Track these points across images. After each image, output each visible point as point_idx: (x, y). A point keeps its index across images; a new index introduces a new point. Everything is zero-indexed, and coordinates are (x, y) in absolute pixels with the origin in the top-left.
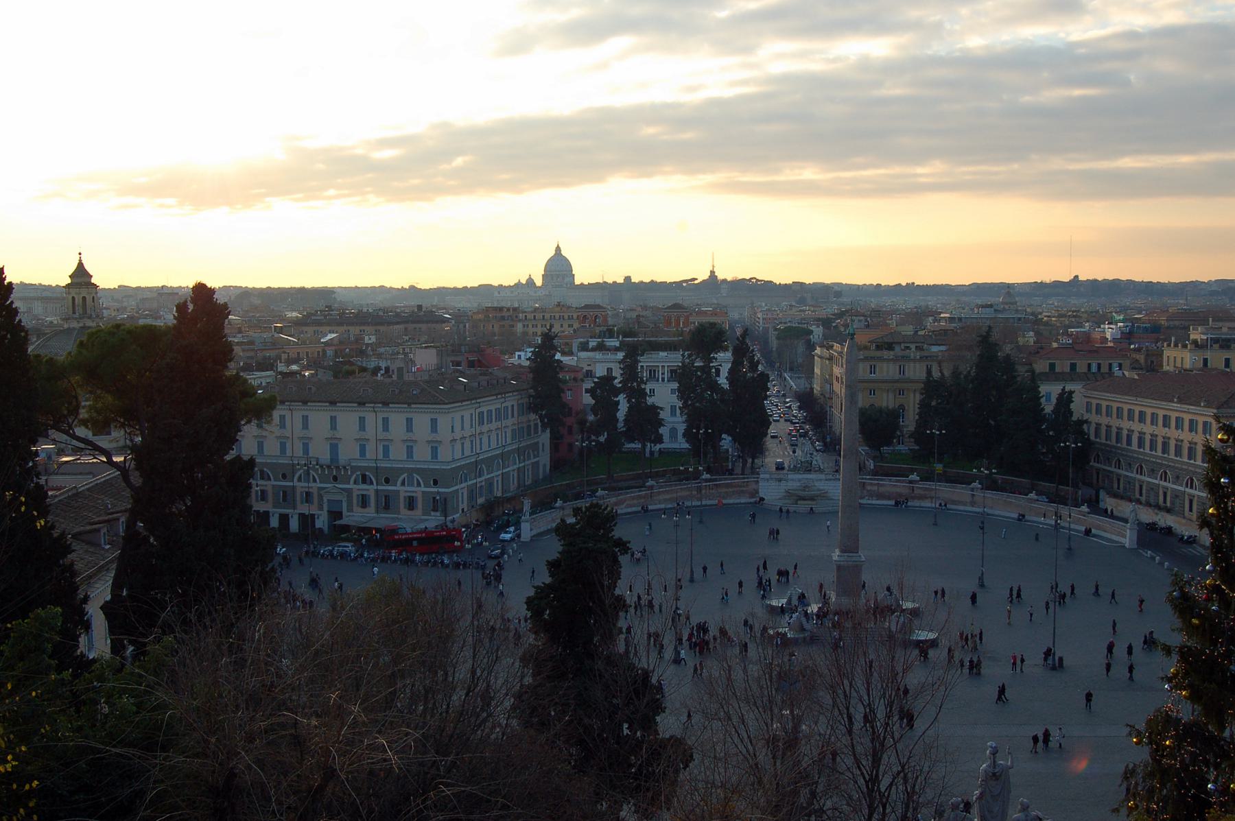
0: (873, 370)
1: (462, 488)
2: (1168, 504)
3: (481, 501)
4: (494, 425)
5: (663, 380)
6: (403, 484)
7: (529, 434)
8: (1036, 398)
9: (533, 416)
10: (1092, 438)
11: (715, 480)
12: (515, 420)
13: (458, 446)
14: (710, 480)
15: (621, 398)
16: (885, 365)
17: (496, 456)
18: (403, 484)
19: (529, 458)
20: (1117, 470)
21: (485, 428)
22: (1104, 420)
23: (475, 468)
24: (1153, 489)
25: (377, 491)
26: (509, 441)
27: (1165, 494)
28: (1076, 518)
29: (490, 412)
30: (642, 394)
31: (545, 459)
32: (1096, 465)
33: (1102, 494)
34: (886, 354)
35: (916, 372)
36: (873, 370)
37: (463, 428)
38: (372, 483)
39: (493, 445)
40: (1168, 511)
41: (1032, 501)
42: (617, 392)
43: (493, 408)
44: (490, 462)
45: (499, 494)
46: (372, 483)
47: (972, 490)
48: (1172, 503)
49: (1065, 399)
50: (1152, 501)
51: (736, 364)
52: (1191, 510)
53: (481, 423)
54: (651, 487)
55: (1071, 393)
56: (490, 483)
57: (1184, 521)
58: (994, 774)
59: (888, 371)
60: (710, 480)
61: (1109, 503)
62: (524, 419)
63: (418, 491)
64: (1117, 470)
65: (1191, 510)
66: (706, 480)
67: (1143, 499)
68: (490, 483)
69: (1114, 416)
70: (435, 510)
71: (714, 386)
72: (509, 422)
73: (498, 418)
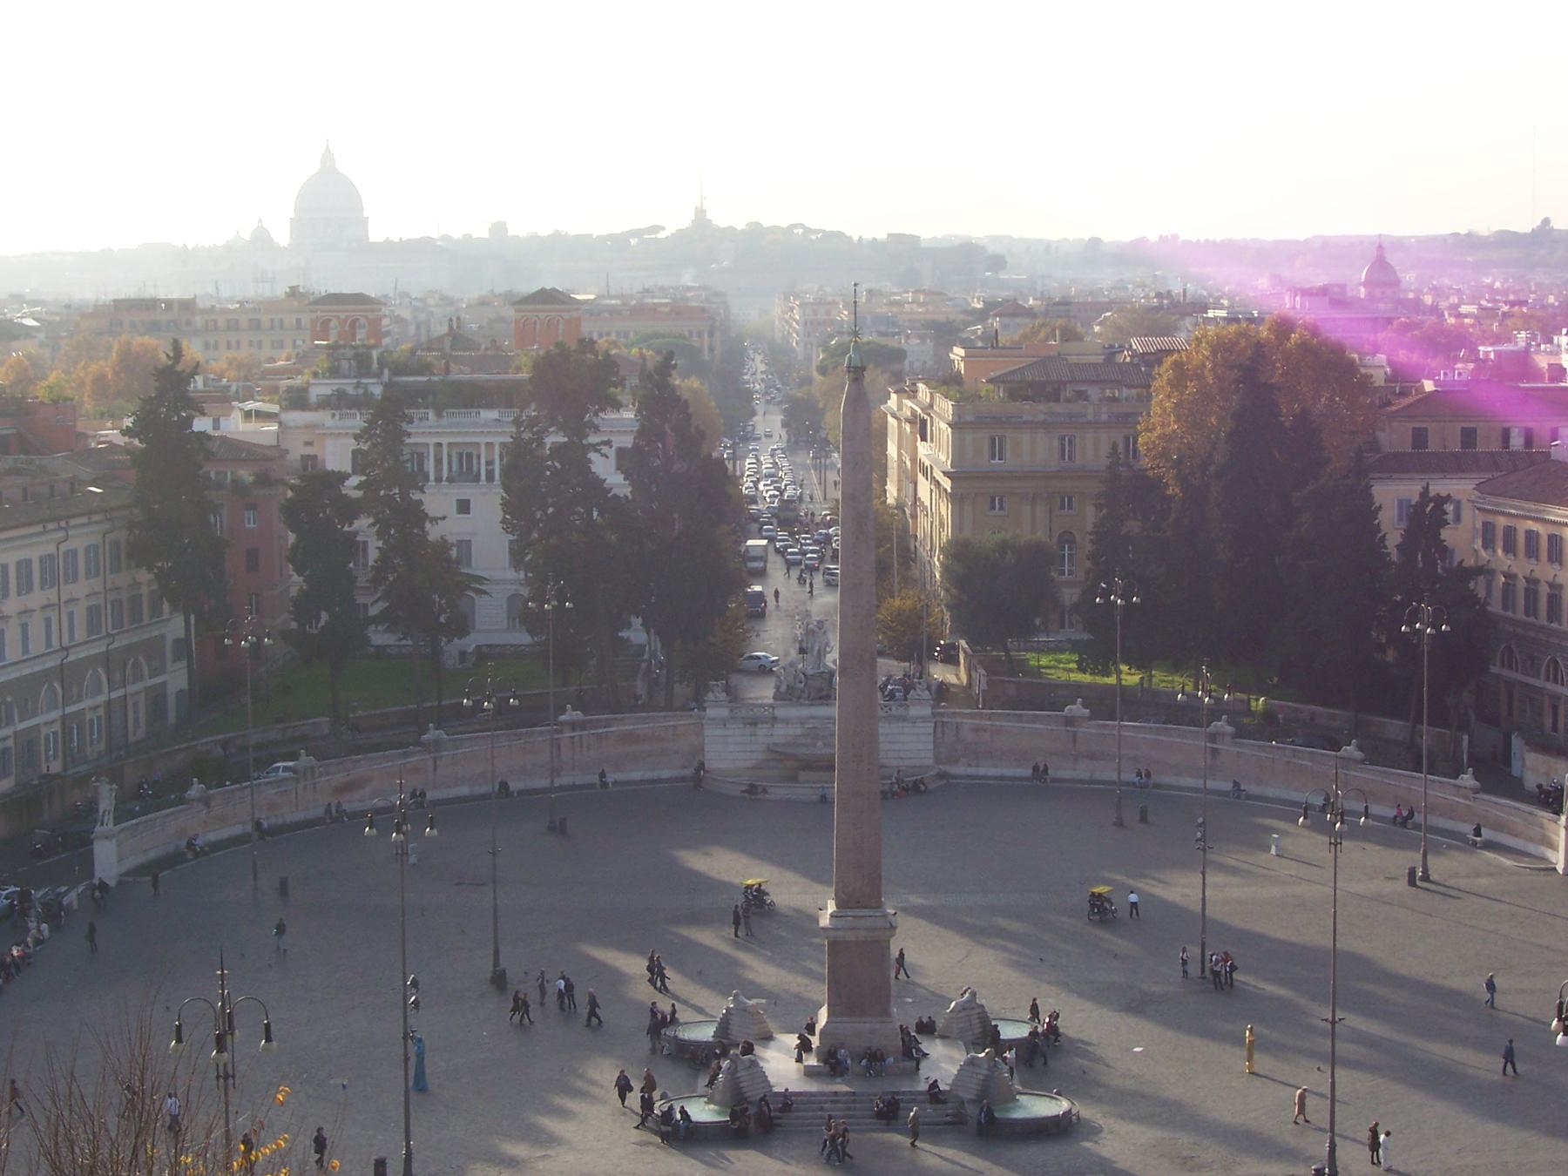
4: (37, 598)
5: (490, 477)
8: (1367, 512)
9: (144, 576)
10: (1495, 607)
12: (96, 584)
14: (582, 725)
15: (363, 523)
17: (45, 675)
19: (138, 677)
20: (1550, 686)
22: (1521, 567)
26: (80, 634)
29: (23, 566)
30: (415, 516)
31: (176, 679)
32: (1506, 672)
33: (1517, 742)
35: (1093, 451)
39: (37, 646)
41: (1348, 760)
42: (351, 510)
43: (35, 554)
45: (56, 767)
47: (1213, 738)
49: (1427, 519)
51: (647, 432)
54: (437, 745)
55: (1441, 501)
60: (582, 725)
61: (1533, 767)
64: (1550, 686)
66: (574, 725)
68: (28, 742)
69: (1544, 555)
71: (596, 487)
72: (81, 588)
73: (49, 580)
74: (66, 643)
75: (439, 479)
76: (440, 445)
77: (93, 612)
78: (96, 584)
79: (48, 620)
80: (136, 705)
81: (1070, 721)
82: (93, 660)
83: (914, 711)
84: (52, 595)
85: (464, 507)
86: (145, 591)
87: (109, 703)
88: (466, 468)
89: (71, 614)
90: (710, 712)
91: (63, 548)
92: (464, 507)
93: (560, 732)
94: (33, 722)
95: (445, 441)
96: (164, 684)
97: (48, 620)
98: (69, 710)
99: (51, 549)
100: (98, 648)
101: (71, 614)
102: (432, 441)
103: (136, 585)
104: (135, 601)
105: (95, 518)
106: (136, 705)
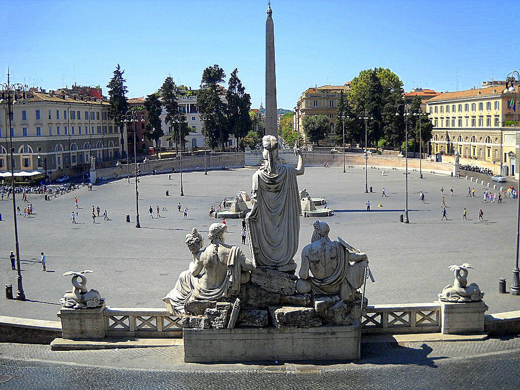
1: (59, 154)
2: (476, 155)
3: (72, 164)
6: (22, 152)
7: (111, 132)
13: (54, 129)
18: (22, 152)
21: (76, 121)
22: (439, 115)
23: (69, 144)
25: (7, 156)
26: (95, 132)
28: (425, 165)
31: (120, 147)
37: (58, 118)
38: (4, 153)
39: (83, 131)
44: (81, 143)
46: (4, 153)
48: (479, 154)
53: (73, 117)
56: (81, 156)
59: (325, 103)
62: (107, 121)
63: (30, 156)
70: (40, 166)
72: (96, 121)
75: (188, 112)
77: (99, 128)
79: (86, 127)
80: (111, 152)
81: (332, 153)
85: (194, 118)
86: (113, 126)
87: (103, 150)
88: (193, 109)
92: (194, 118)
94: (82, 151)
96: (119, 149)
97: (86, 127)
100: (100, 136)
106: (111, 152)
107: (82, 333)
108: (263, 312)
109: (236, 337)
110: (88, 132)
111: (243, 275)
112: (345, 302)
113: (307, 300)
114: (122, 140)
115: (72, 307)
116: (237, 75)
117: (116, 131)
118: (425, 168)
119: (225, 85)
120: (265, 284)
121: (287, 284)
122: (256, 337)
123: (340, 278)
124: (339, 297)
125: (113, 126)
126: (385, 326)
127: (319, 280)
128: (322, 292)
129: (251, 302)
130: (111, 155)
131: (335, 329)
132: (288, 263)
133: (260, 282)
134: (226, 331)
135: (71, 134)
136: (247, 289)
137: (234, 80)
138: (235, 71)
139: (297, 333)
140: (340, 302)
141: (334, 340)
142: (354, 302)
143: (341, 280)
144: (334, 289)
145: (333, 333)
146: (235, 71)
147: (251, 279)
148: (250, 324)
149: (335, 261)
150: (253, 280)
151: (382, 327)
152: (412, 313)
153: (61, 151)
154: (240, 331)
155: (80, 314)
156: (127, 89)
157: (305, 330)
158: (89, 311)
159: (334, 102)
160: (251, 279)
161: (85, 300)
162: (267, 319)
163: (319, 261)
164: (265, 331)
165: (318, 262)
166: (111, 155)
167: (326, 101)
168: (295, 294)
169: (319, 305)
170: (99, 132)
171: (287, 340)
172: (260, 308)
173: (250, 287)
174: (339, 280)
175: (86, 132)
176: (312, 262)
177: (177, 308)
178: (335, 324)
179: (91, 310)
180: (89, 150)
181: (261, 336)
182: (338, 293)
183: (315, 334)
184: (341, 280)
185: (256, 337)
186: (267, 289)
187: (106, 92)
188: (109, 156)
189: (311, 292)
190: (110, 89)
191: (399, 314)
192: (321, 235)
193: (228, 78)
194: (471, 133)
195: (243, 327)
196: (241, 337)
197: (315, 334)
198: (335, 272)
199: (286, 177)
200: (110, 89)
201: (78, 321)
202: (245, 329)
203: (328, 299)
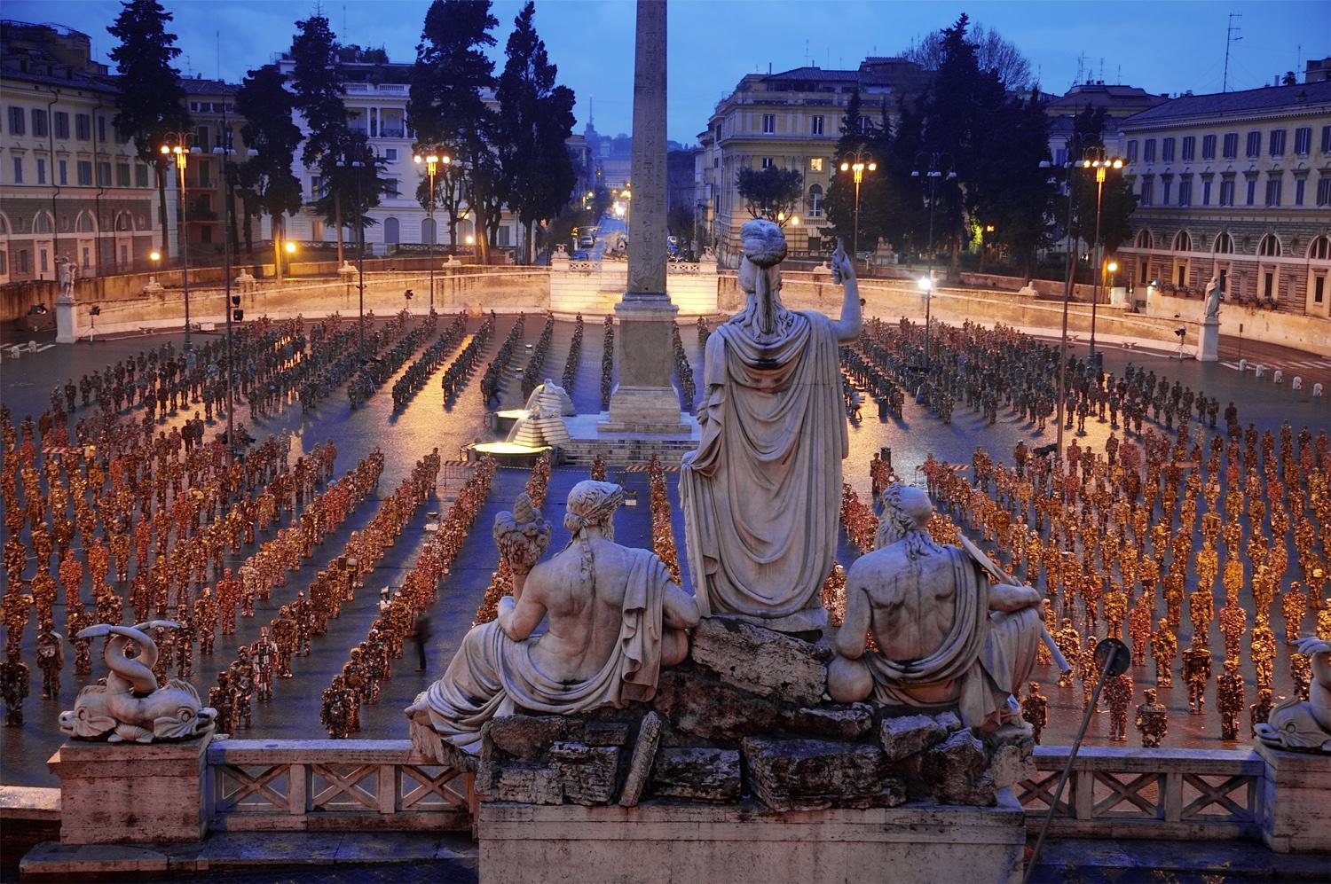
0: (769, 123)
2: (1275, 295)
7: (124, 180)
11: (471, 270)
16: (790, 117)
17: (39, 204)
24: (1247, 272)
26: (72, 179)
27: (1269, 278)
34: (792, 97)
36: (769, 123)
40: (1276, 307)
48: (1283, 291)
50: (1244, 291)
52: (1319, 298)
57: (1304, 320)
58: (766, 362)
65: (1319, 298)
66: (454, 270)
67: (1228, 294)
74: (58, 183)
75: (374, 134)
76: (375, 110)
77: (84, 168)
78: (88, 146)
81: (817, 277)
82: (83, 204)
83: (704, 268)
84: (45, 142)
89: (63, 164)
90: (555, 266)
91: (56, 108)
93: (445, 274)
95: (378, 107)
97: (41, 163)
98: (60, 236)
99: (43, 107)
100: (89, 195)
101: (63, 164)
102: (369, 106)
103: (123, 156)
104: (123, 169)
105: (84, 94)
106: (124, 248)
107: (131, 821)
108: (725, 755)
109: (641, 832)
110: (48, 182)
111: (669, 639)
112: (977, 732)
113: (862, 722)
114: (163, 209)
115: (103, 738)
116: (537, 22)
117: (142, 180)
118: (1107, 331)
119: (497, 56)
120: (733, 669)
121: (798, 672)
122: (705, 832)
123: (962, 658)
124: (960, 717)
125: (132, 163)
126: (1083, 811)
127: (899, 663)
128: (905, 698)
129: (687, 723)
130: (124, 258)
131: (946, 815)
132: (803, 609)
133: (720, 661)
134: (614, 813)
135: (58, 183)
136: (680, 682)
137: (525, 41)
138: (529, 10)
139: (835, 824)
140: (963, 733)
141: (942, 850)
142: (1000, 735)
143: (963, 665)
144: (941, 693)
145: (942, 828)
146: (529, 10)
147: (690, 652)
148: (688, 792)
149: (948, 607)
150: (698, 655)
151: (1075, 818)
152: (1170, 777)
153: (92, 230)
154: (654, 813)
155: (129, 762)
156: (175, 44)
157: (855, 816)
158: (163, 753)
159: (826, 120)
160: (690, 652)
161: (148, 715)
162: (738, 775)
163: (902, 603)
164: (731, 815)
165: (897, 607)
166: (124, 258)
167: (800, 116)
168: (824, 705)
169: (901, 739)
170: (84, 177)
171: (801, 845)
172: (719, 740)
173: (687, 675)
174: (957, 664)
175: (42, 179)
176: (881, 606)
177: (456, 739)
178: (945, 800)
179: (167, 747)
180: (50, 236)
181: (721, 831)
182: (954, 705)
183: (887, 828)
184: (963, 665)
185: (705, 832)
186: (737, 684)
187: (104, 47)
188: (119, 260)
189: (869, 698)
190: (117, 42)
191: (1126, 779)
192: (905, 527)
193: (503, 31)
194: (1264, 225)
195: (666, 801)
196: (658, 831)
197: (887, 828)
198: (948, 641)
199: (808, 343)
200: (117, 42)
201: (119, 786)
202: (672, 809)
203: (925, 722)
